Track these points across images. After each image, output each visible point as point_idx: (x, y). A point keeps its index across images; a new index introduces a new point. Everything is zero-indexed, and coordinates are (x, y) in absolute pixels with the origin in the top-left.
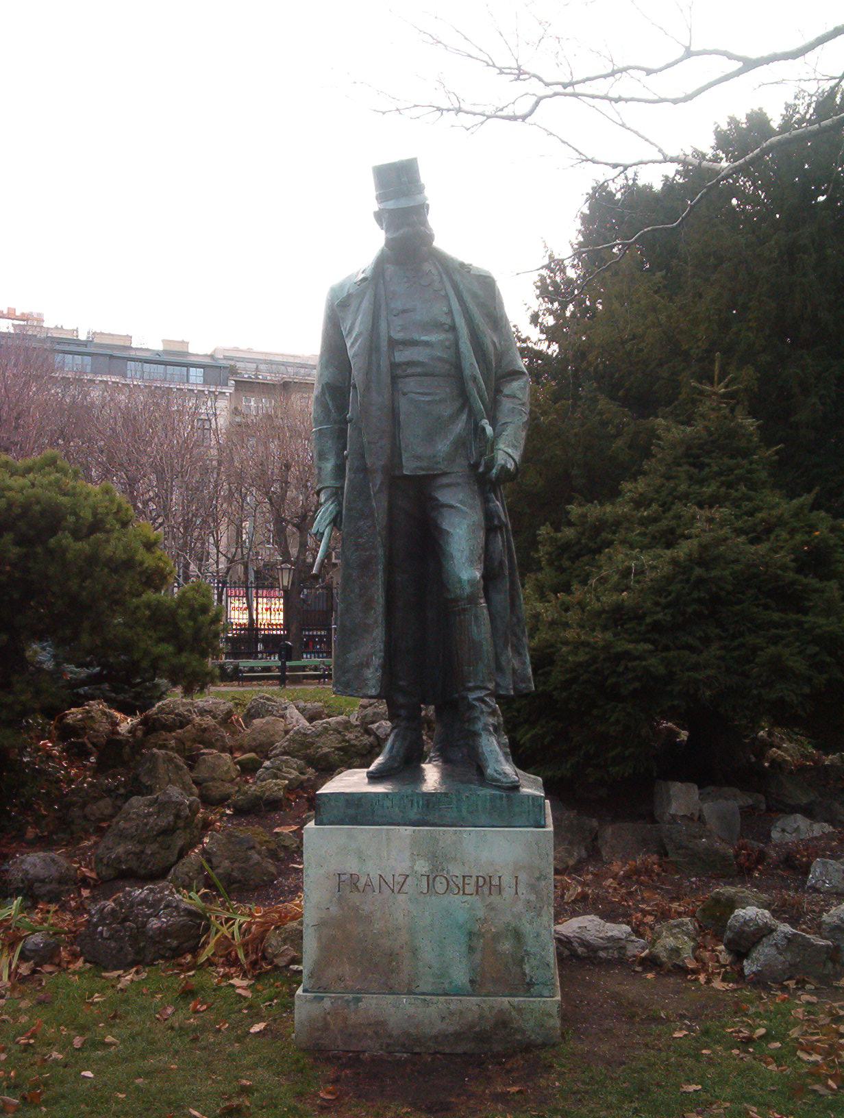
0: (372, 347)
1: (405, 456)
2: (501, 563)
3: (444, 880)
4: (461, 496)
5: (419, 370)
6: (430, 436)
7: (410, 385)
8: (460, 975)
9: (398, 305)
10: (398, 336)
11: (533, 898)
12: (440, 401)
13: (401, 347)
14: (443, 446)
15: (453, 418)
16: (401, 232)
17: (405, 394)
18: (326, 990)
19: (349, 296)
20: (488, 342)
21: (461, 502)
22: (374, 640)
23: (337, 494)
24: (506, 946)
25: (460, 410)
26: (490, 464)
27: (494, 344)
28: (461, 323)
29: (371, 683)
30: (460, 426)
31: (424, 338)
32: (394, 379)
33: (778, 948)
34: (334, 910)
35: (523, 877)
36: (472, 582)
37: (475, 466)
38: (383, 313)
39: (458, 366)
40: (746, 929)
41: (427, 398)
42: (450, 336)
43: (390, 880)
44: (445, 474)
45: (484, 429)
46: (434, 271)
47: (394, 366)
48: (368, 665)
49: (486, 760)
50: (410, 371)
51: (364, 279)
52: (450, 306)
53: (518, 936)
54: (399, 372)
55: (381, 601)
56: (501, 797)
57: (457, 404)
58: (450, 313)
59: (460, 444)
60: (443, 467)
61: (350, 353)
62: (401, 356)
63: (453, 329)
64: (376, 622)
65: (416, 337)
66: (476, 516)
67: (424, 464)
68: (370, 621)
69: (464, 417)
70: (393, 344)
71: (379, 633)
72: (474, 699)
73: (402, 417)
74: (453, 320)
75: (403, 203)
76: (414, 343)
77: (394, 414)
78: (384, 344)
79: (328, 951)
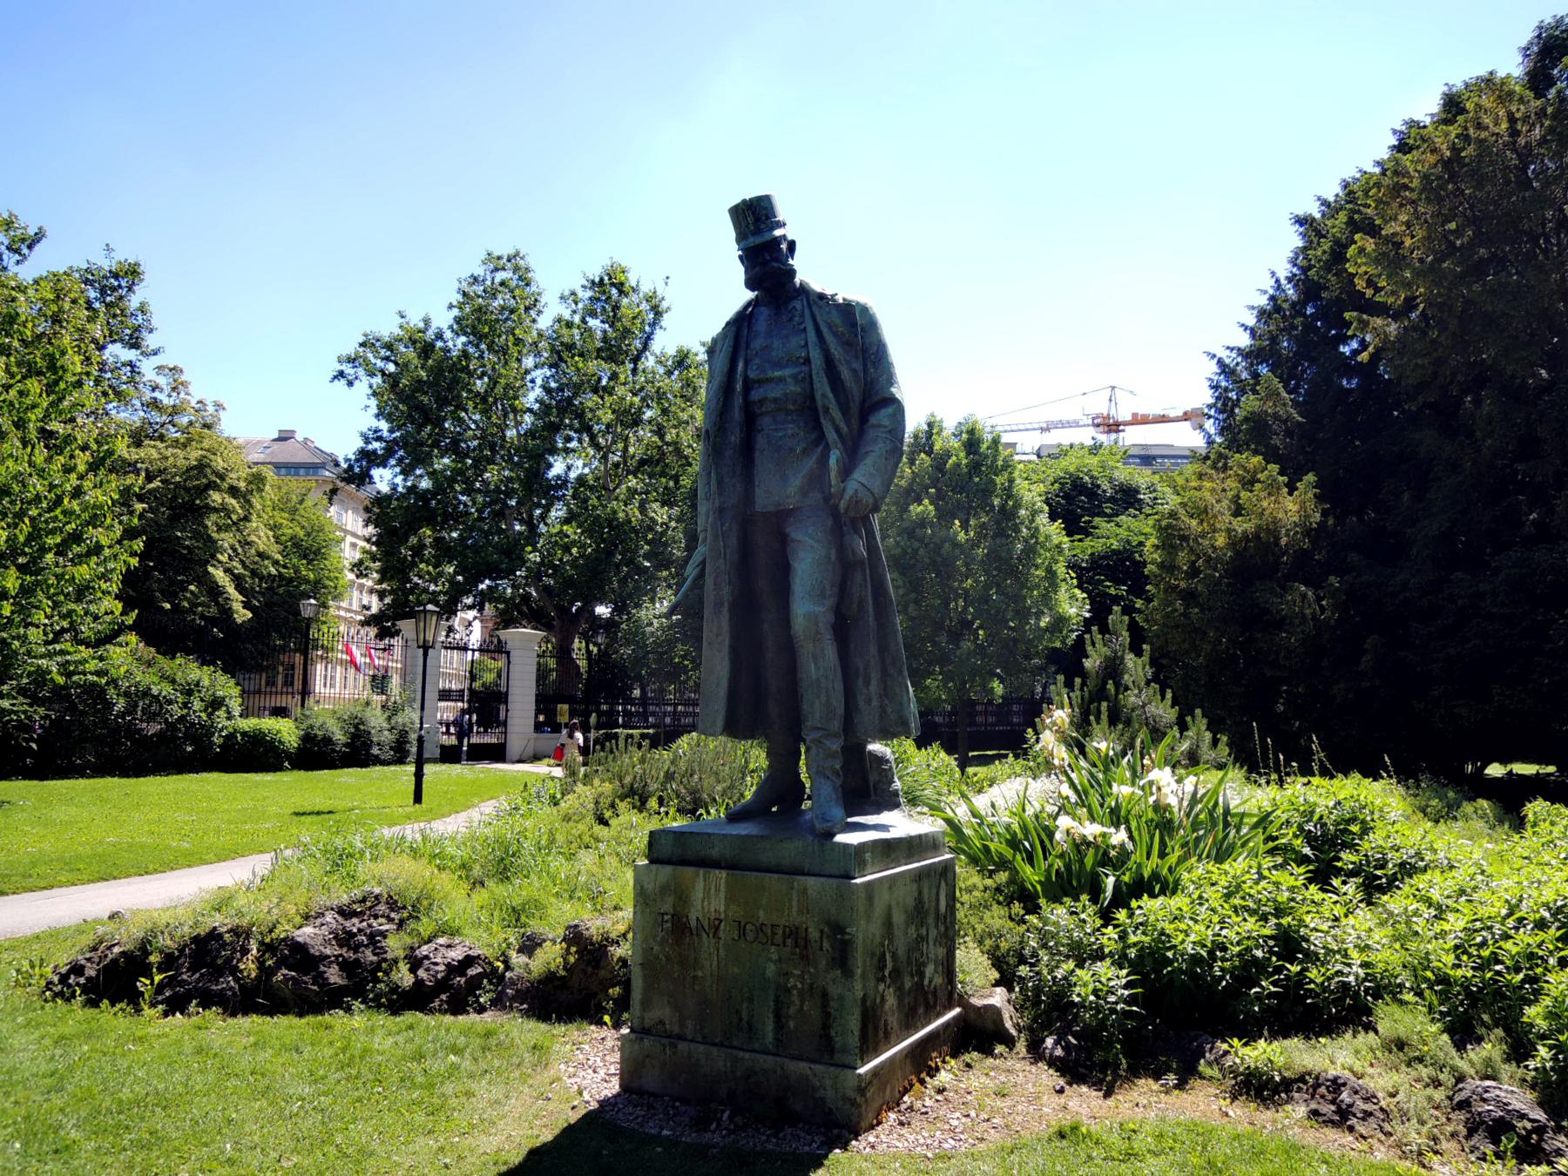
31: (777, 374)
63: (807, 361)
65: (770, 374)
73: (757, 454)
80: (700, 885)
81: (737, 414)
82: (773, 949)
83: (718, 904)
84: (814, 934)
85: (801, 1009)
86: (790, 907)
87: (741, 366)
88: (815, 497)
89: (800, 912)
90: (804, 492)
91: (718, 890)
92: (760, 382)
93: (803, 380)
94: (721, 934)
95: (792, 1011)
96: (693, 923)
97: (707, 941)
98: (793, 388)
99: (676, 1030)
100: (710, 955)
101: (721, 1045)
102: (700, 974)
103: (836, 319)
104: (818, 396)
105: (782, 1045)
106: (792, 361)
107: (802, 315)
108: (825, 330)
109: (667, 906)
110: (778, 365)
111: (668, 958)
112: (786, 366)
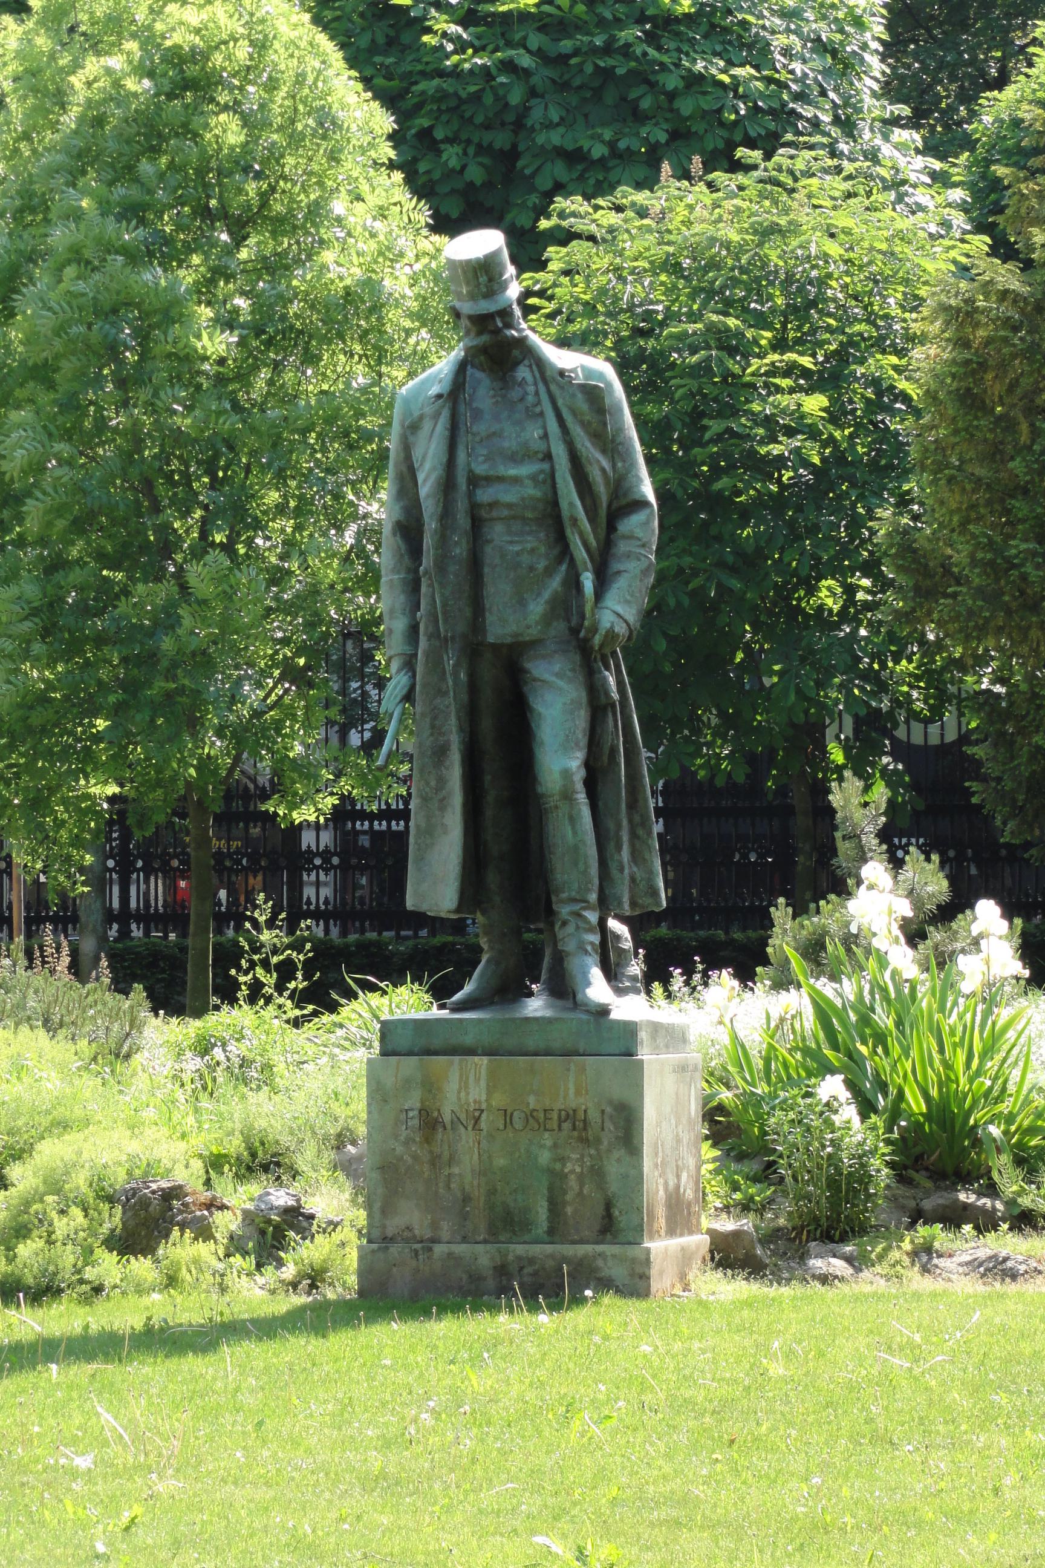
0: (447, 485)
2: (614, 751)
4: (557, 667)
5: (506, 513)
10: (480, 469)
14: (537, 608)
15: (549, 572)
19: (421, 418)
25: (559, 561)
27: (603, 470)
30: (555, 583)
31: (512, 472)
39: (554, 503)
41: (517, 548)
42: (546, 466)
43: (463, 1117)
51: (439, 396)
52: (545, 428)
57: (556, 551)
58: (545, 436)
62: (484, 495)
63: (548, 457)
69: (564, 567)
70: (474, 481)
73: (486, 570)
75: (485, 307)
76: (501, 479)
80: (454, 1076)
81: (463, 520)
82: (547, 1135)
84: (594, 1115)
85: (580, 1194)
87: (461, 456)
88: (559, 627)
89: (578, 1093)
90: (547, 619)
91: (477, 1080)
92: (489, 480)
93: (544, 482)
95: (568, 1197)
96: (447, 1117)
97: (467, 1139)
98: (531, 491)
99: (428, 1234)
100: (468, 1154)
101: (485, 1242)
102: (456, 1170)
104: (564, 505)
105: (555, 1233)
107: (537, 393)
109: (414, 1101)
110: (514, 458)
111: (415, 1158)
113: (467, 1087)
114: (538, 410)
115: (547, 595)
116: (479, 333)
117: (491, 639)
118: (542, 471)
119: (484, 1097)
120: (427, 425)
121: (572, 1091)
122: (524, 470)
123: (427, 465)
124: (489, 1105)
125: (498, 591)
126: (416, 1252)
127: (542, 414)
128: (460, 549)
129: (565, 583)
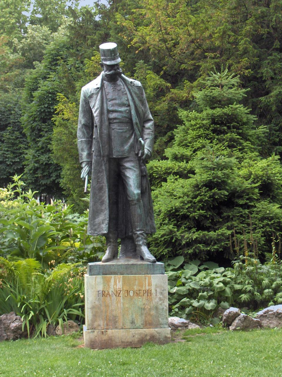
0: (101, 113)
1: (114, 151)
3: (133, 292)
4: (133, 164)
5: (118, 121)
6: (122, 144)
7: (115, 126)
8: (139, 322)
9: (109, 97)
10: (111, 108)
11: (161, 296)
12: (125, 132)
13: (111, 113)
15: (130, 137)
16: (112, 72)
17: (113, 129)
18: (95, 329)
20: (140, 110)
21: (133, 166)
22: (105, 214)
23: (89, 164)
24: (153, 312)
26: (143, 154)
28: (131, 103)
29: (104, 229)
30: (131, 140)
31: (120, 110)
32: (110, 123)
33: (241, 321)
34: (97, 303)
35: (158, 290)
36: (138, 194)
37: (137, 154)
38: (105, 100)
39: (131, 119)
40: (230, 315)
41: (121, 131)
42: (128, 108)
44: (127, 157)
45: (140, 142)
46: (121, 84)
47: (109, 119)
48: (103, 223)
49: (144, 254)
50: (115, 121)
52: (127, 97)
53: (157, 308)
54: (111, 121)
55: (108, 201)
56: (150, 265)
58: (128, 100)
59: (132, 147)
60: (126, 155)
61: (95, 115)
63: (129, 106)
64: (106, 208)
66: (138, 172)
67: (121, 154)
68: (103, 208)
69: (133, 137)
70: (109, 111)
71: (107, 212)
72: (140, 234)
73: (113, 137)
74: (129, 103)
77: (109, 136)
78: (105, 111)
79: (95, 316)
80: (112, 281)
81: (107, 123)
83: (119, 285)
86: (146, 284)
89: (149, 285)
91: (119, 282)
93: (128, 113)
94: (121, 295)
103: (136, 90)
106: (123, 105)
107: (124, 88)
108: (133, 94)
112: (122, 107)
113: (116, 284)
114: (125, 92)
115: (129, 144)
116: (110, 71)
117: (114, 157)
118: (127, 110)
119: (121, 287)
120: (95, 96)
121: (147, 285)
122: (123, 109)
123: (96, 108)
124: (123, 289)
125: (116, 143)
126: (103, 332)
127: (126, 94)
128: (105, 132)
129: (134, 141)
